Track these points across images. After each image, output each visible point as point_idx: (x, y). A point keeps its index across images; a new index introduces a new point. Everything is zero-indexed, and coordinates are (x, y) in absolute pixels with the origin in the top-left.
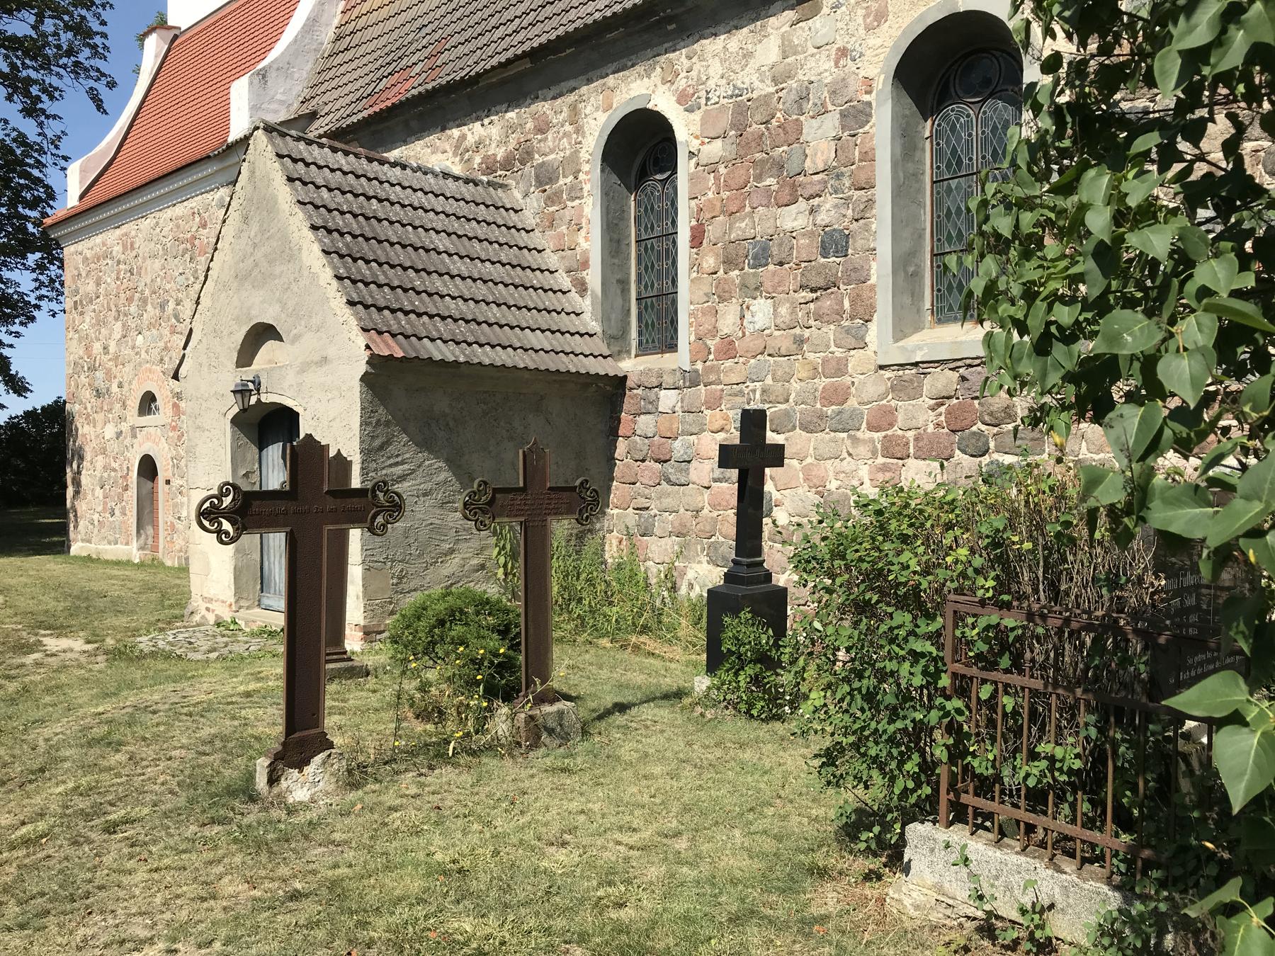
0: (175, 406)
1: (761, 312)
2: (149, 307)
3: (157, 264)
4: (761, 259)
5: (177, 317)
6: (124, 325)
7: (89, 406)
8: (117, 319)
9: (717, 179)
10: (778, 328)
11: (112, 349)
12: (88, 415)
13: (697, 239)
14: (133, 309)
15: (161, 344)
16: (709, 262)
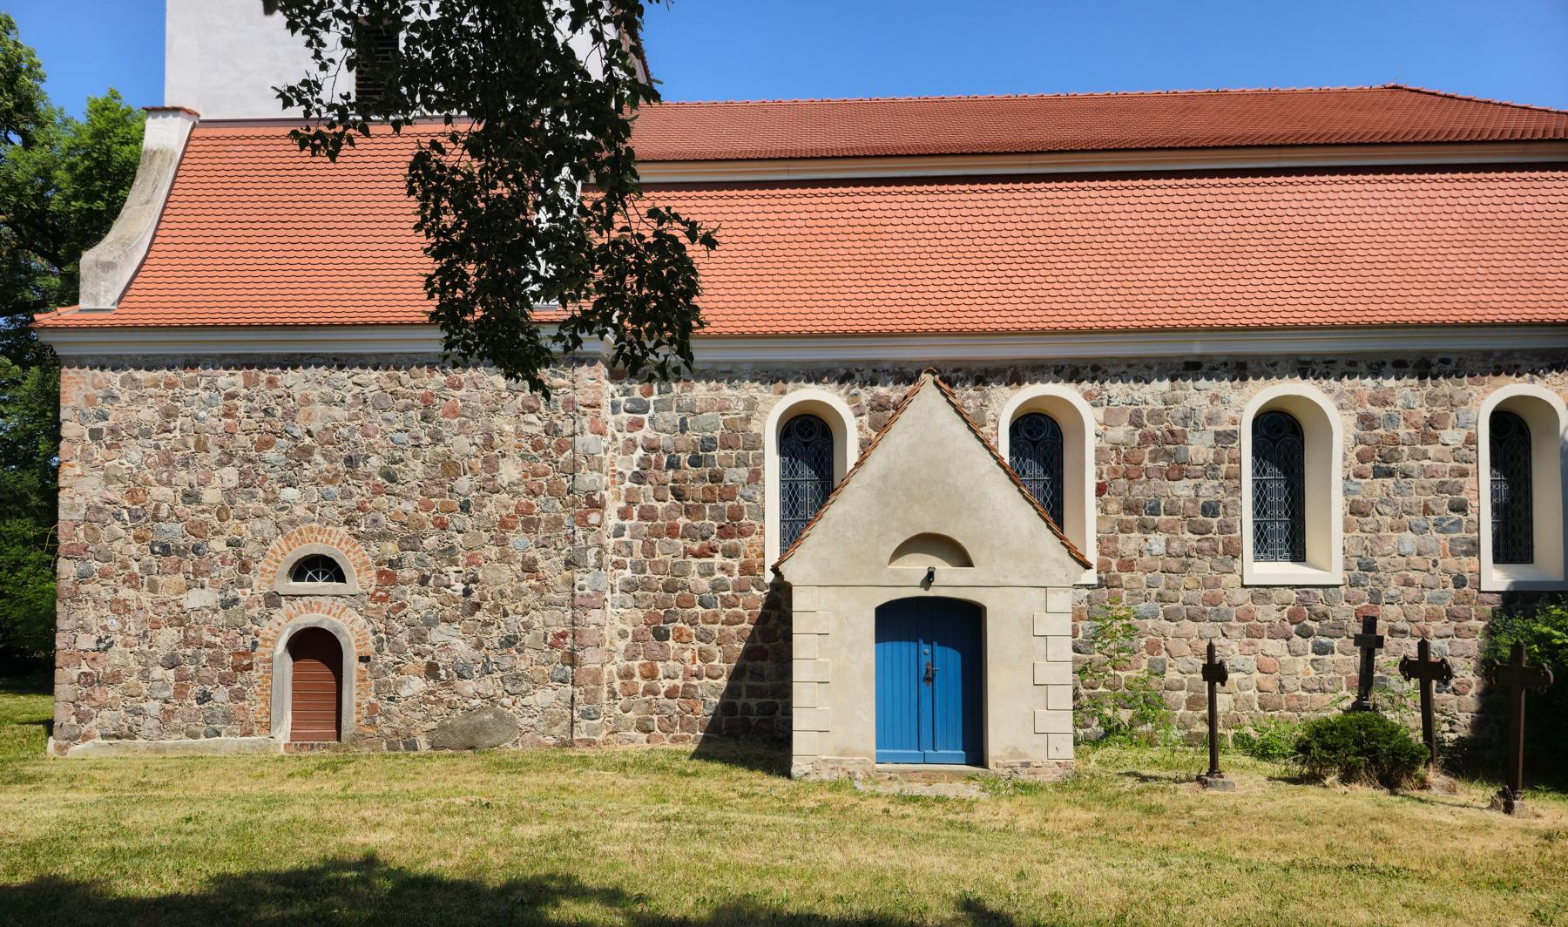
0: (380, 574)
1: (1157, 542)
2: (317, 457)
3: (338, 412)
4: (1155, 511)
5: (391, 478)
6: (243, 474)
7: (135, 567)
8: (221, 464)
9: (1118, 454)
10: (1169, 555)
11: (211, 495)
12: (133, 576)
13: (1101, 490)
14: (270, 454)
15: (352, 503)
16: (1113, 507)
